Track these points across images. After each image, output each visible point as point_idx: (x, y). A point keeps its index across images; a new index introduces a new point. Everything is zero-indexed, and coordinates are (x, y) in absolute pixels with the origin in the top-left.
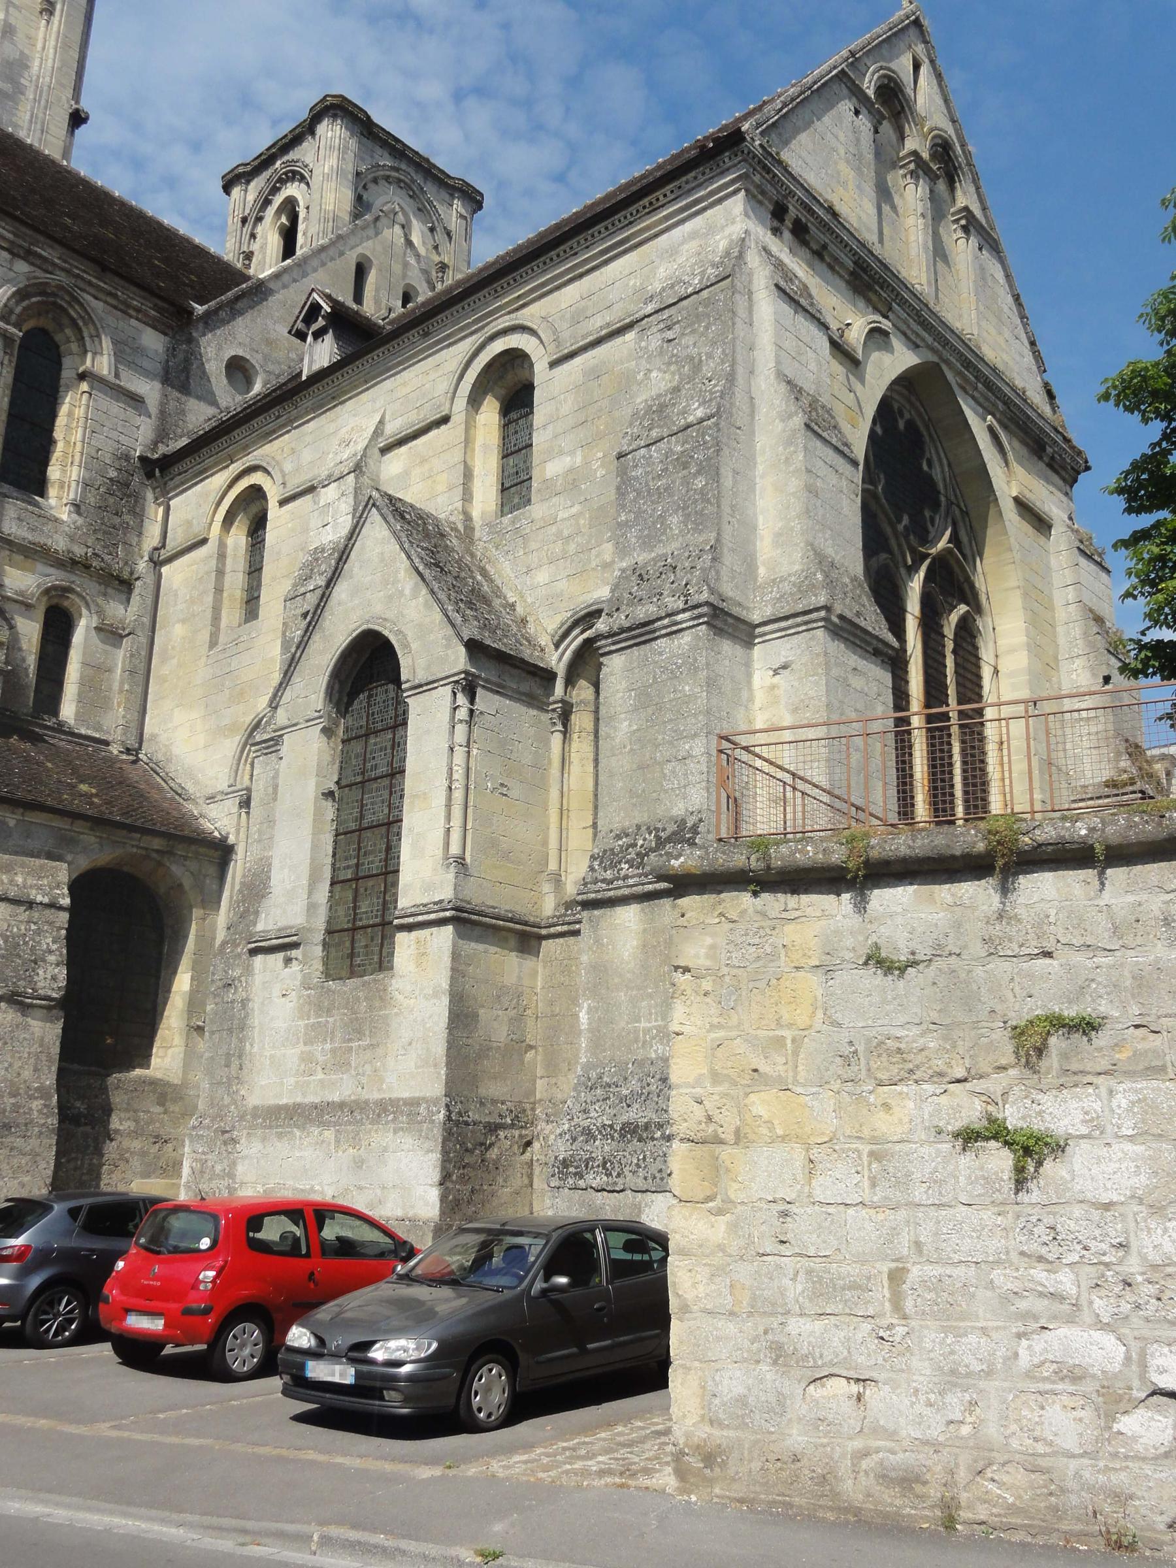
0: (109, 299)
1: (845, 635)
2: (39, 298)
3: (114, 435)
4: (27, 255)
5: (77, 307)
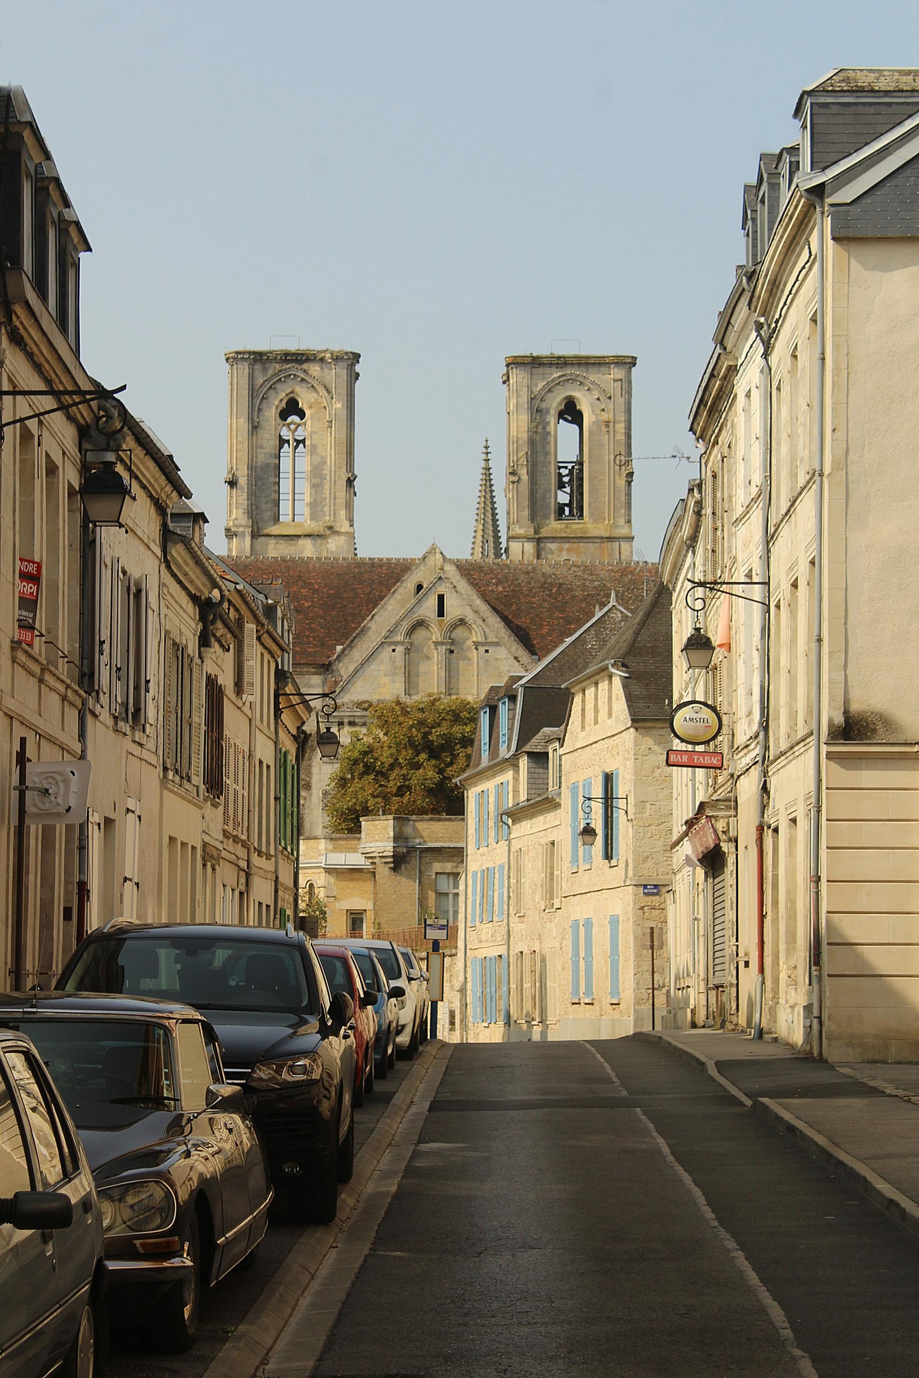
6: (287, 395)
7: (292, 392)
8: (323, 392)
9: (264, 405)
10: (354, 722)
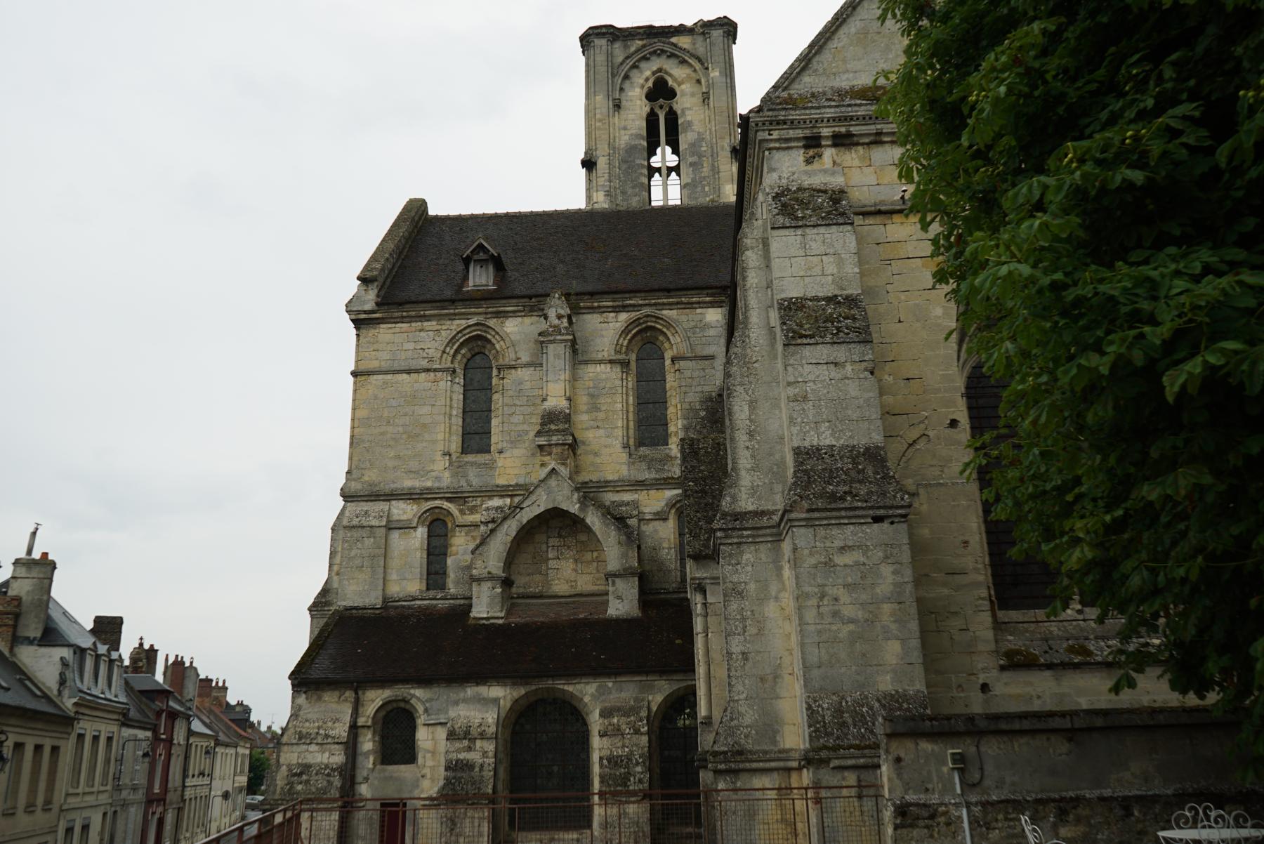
0: (679, 306)
1: (825, 522)
2: (637, 329)
3: (699, 389)
4: (624, 308)
5: (661, 322)
6: (654, 73)
7: (660, 70)
8: (698, 66)
9: (627, 85)
10: (849, 135)
